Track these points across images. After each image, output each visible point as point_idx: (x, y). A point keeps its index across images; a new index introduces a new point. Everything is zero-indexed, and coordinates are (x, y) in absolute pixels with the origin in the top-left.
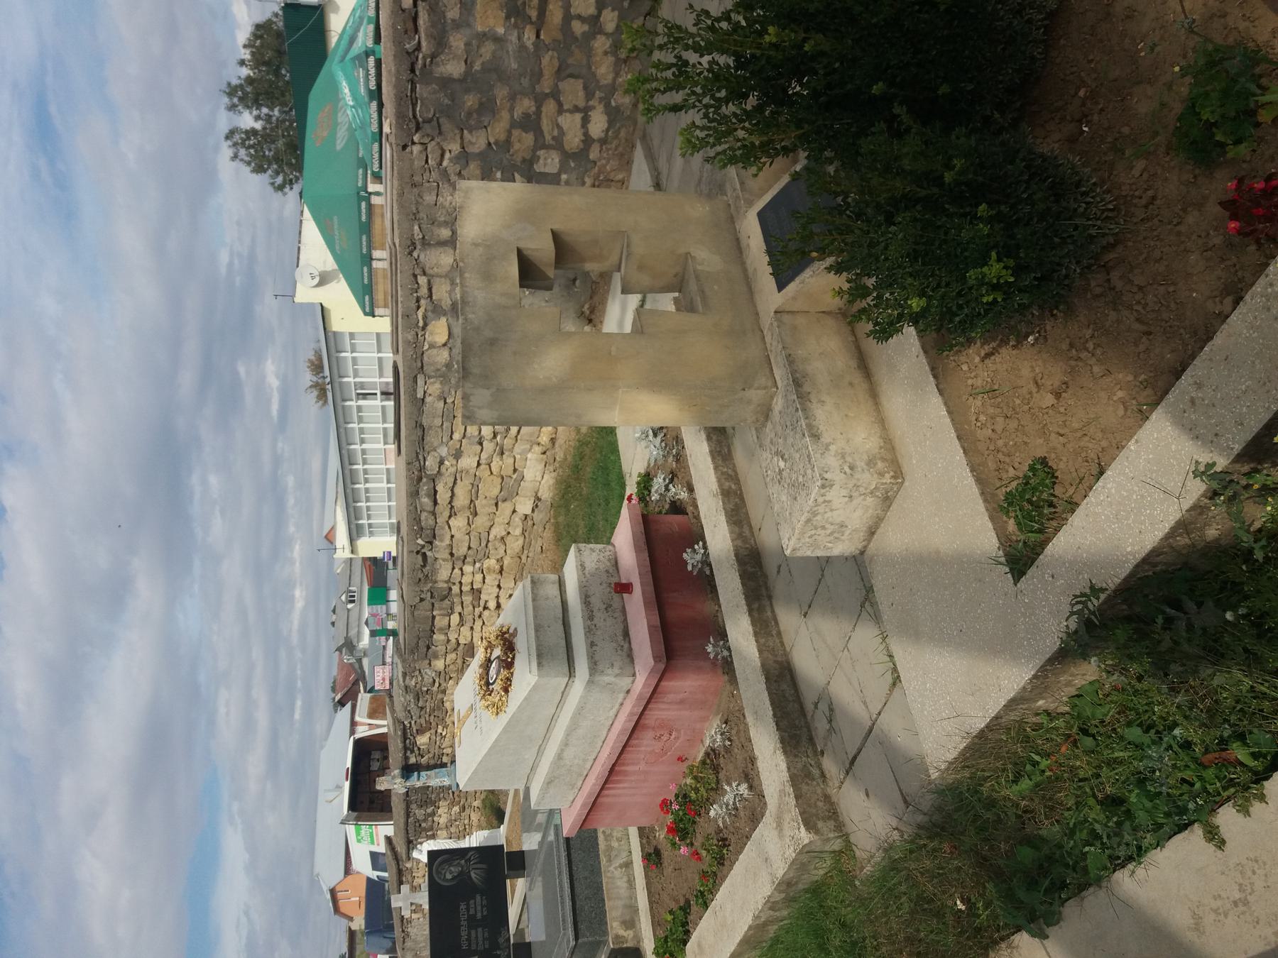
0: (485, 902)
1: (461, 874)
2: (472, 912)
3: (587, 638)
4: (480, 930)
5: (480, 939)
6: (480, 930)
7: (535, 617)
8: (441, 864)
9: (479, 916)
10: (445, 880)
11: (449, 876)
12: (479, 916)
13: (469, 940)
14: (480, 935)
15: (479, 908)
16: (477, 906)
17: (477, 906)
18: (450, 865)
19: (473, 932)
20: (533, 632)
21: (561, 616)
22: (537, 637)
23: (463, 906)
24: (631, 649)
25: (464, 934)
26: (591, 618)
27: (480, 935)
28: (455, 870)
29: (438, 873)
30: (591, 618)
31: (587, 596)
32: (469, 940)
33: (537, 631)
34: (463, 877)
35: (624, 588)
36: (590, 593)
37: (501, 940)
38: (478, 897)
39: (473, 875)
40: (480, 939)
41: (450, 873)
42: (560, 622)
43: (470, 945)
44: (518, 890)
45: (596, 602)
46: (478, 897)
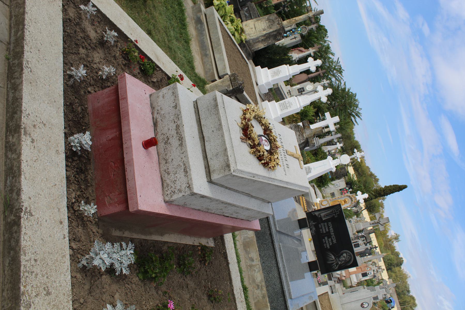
0: (325, 245)
1: (339, 257)
2: (330, 240)
3: (179, 110)
4: (325, 232)
5: (323, 228)
6: (325, 232)
7: (223, 136)
8: (350, 260)
9: (326, 238)
10: (346, 253)
11: (345, 255)
12: (326, 238)
13: (329, 227)
14: (324, 230)
15: (327, 242)
16: (328, 243)
17: (328, 243)
18: (345, 260)
19: (327, 230)
20: (223, 123)
21: (206, 144)
22: (220, 120)
23: (335, 241)
24: (153, 113)
25: (331, 229)
26: (178, 127)
27: (324, 230)
28: (342, 258)
29: (350, 256)
30: (178, 127)
31: (181, 145)
32: (329, 227)
33: (220, 125)
34: (338, 256)
35: (148, 144)
36: (179, 148)
37: (314, 229)
38: (328, 247)
39: (333, 257)
40: (323, 228)
41: (344, 256)
42: (206, 139)
43: (328, 224)
44: (310, 256)
45: (174, 142)
46: (328, 247)
